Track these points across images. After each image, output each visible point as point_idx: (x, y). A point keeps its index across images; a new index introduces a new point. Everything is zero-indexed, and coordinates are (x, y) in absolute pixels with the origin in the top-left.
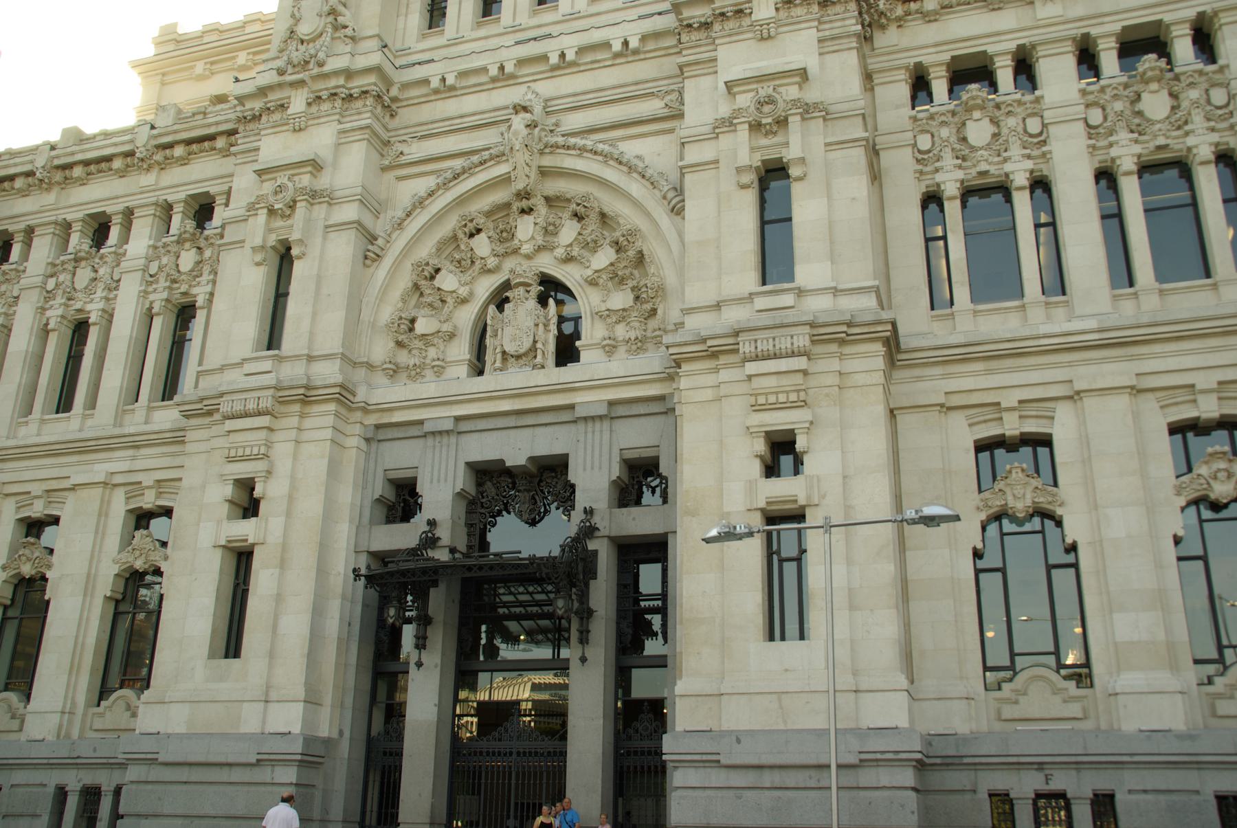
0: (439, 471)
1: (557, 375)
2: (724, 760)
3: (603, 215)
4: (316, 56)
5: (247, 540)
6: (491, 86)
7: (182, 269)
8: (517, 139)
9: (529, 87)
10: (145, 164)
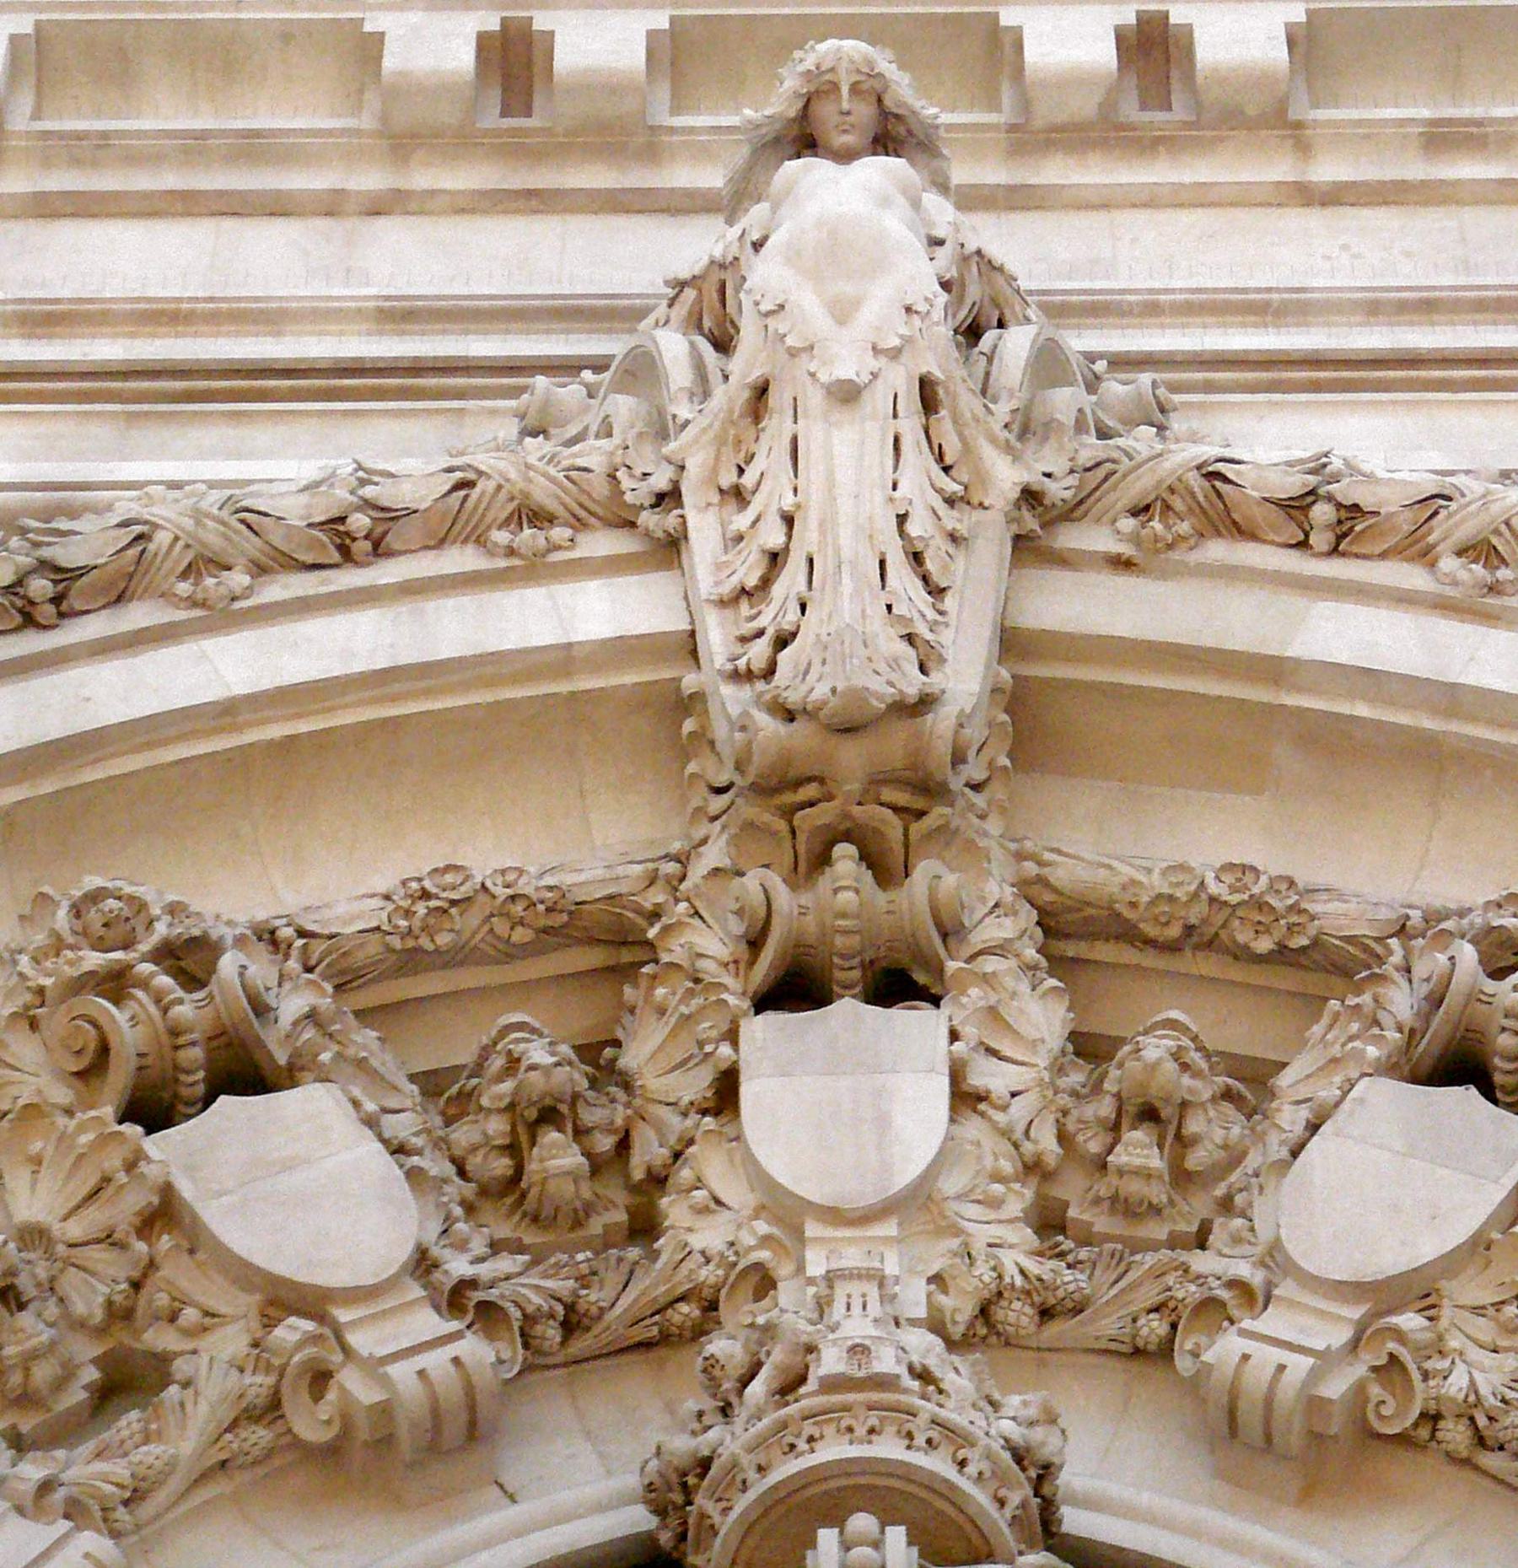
6: (371, 180)
8: (842, 312)
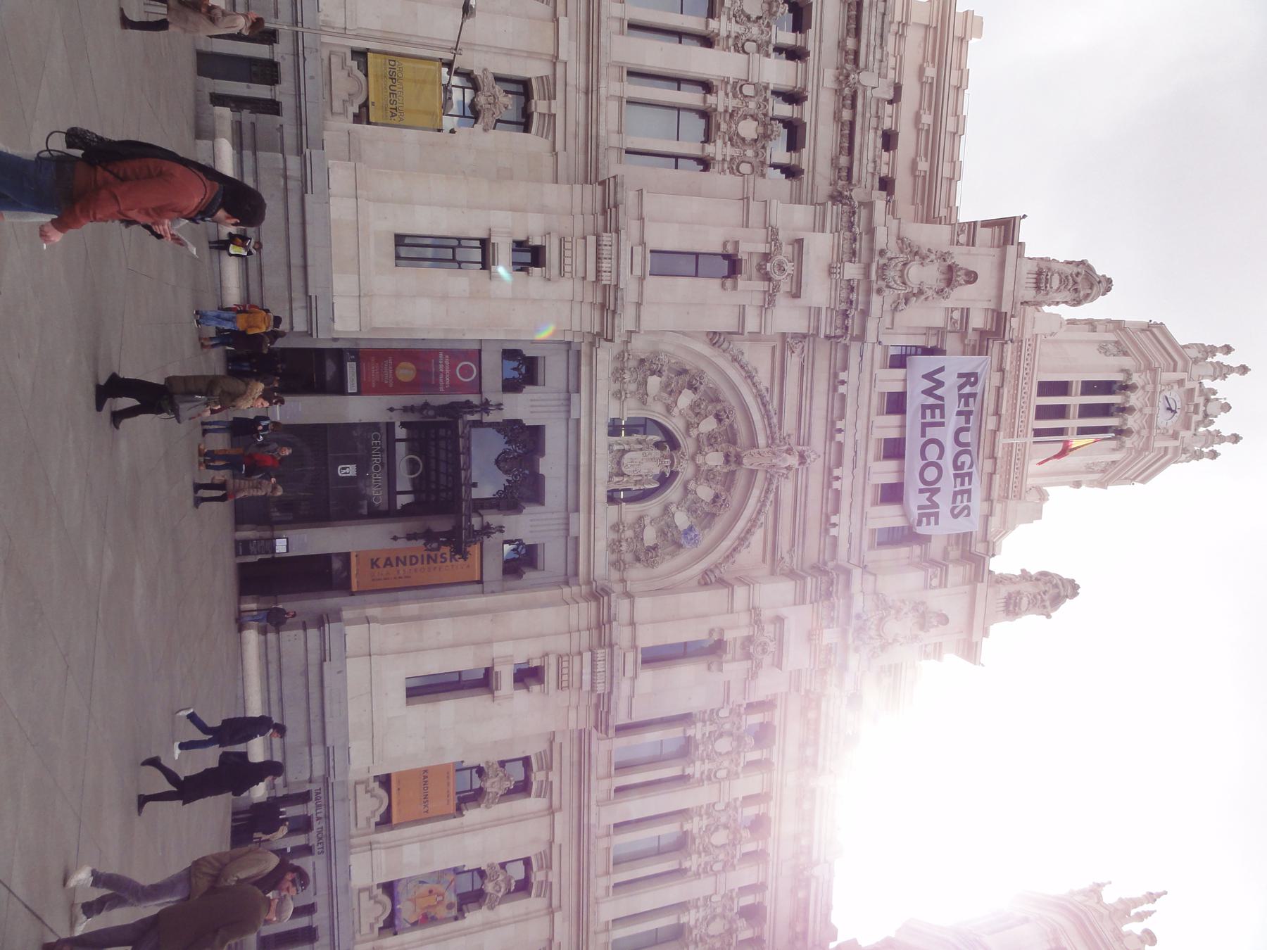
0: (540, 406)
1: (601, 493)
2: (326, 665)
3: (714, 515)
4: (888, 287)
5: (494, 265)
6: (829, 419)
7: (742, 124)
9: (819, 456)
10: (843, 78)
